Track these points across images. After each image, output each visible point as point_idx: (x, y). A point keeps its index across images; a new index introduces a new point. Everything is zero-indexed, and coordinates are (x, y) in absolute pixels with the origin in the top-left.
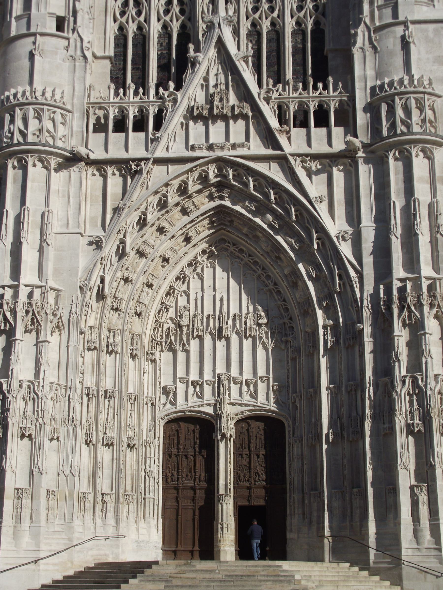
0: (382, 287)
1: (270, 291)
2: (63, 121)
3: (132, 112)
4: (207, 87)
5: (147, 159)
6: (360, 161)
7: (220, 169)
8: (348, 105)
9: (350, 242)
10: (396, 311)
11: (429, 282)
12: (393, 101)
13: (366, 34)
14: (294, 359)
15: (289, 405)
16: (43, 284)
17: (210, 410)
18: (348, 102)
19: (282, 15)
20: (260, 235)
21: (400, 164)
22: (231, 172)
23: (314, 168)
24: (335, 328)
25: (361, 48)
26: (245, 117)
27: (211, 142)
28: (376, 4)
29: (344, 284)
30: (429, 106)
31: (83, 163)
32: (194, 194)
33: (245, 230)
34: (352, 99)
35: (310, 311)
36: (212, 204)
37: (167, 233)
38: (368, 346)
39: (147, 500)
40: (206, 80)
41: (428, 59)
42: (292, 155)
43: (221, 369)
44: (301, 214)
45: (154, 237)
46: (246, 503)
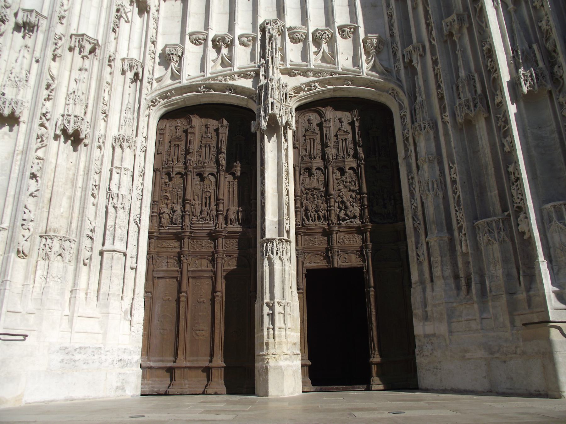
15: (398, 71)
39: (106, 255)
46: (321, 263)
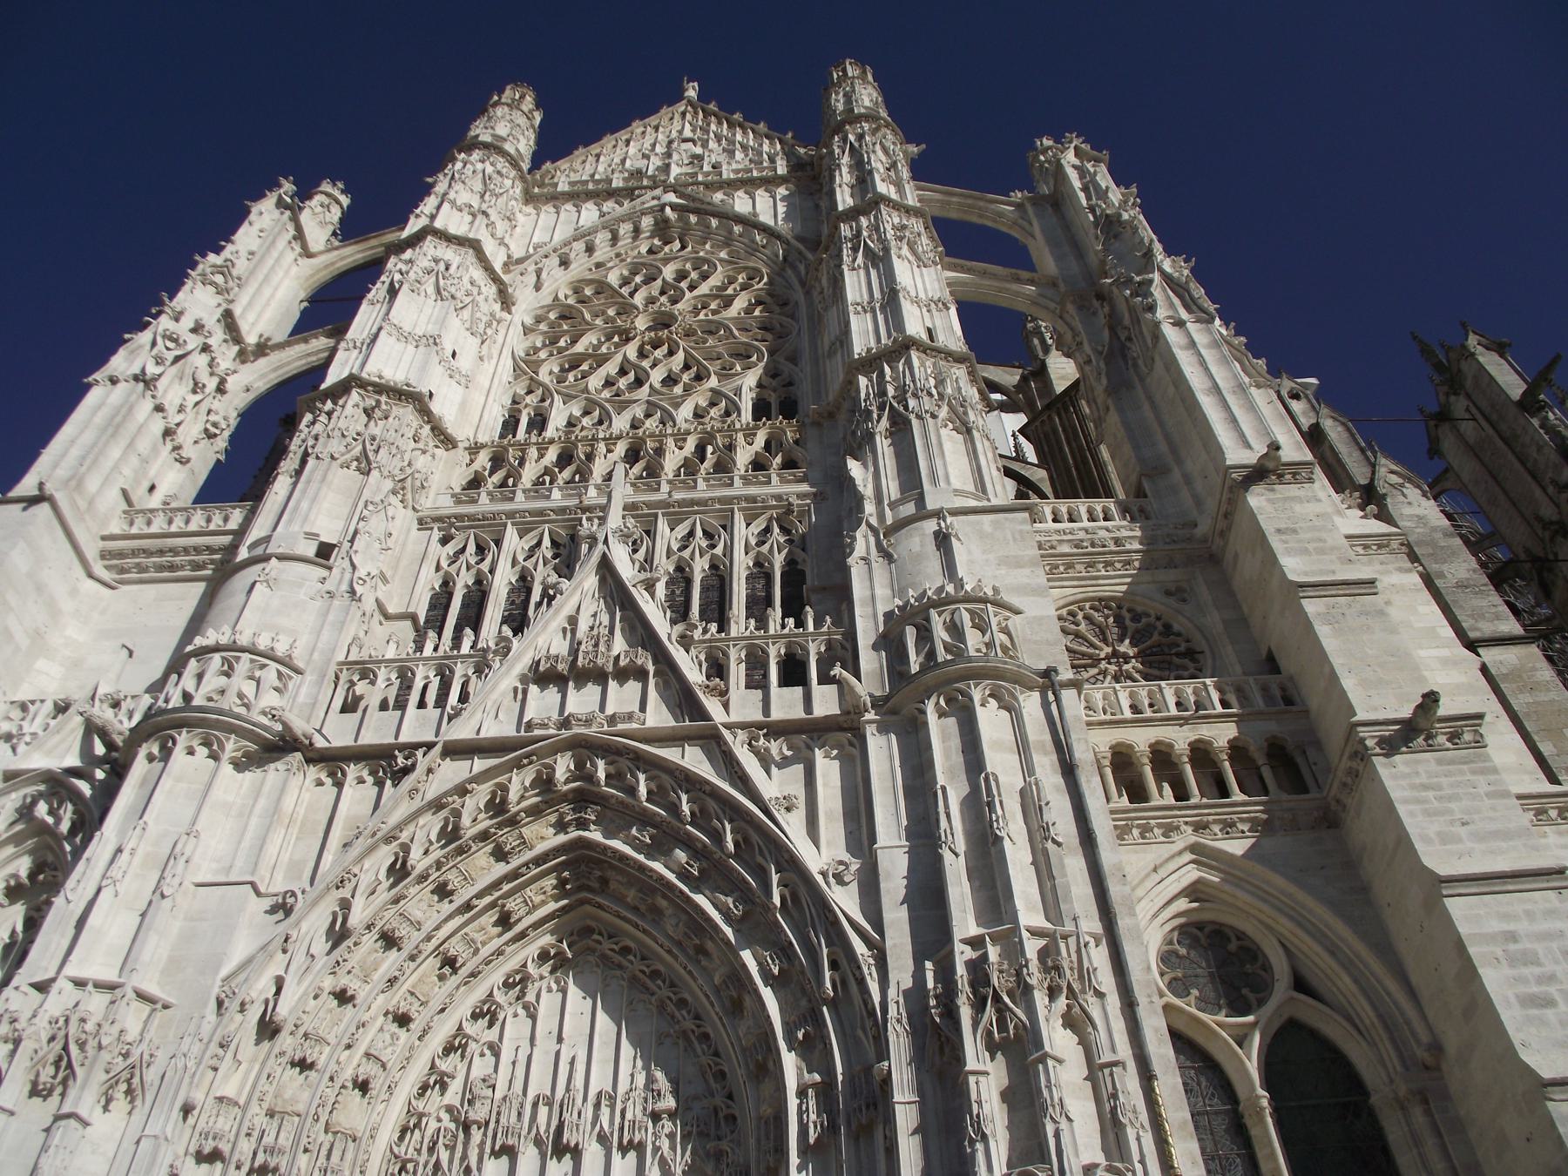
0: (929, 965)
2: (281, 686)
4: (574, 632)
5: (430, 746)
6: (870, 730)
7: (580, 765)
8: (843, 647)
9: (854, 887)
10: (966, 1013)
11: (1042, 942)
12: (928, 620)
13: (872, 540)
18: (844, 642)
19: (729, 550)
20: (664, 903)
21: (951, 722)
22: (601, 764)
23: (774, 752)
24: (826, 1092)
25: (863, 559)
26: (641, 675)
28: (886, 502)
29: (844, 982)
30: (999, 624)
31: (298, 755)
32: (523, 814)
34: (851, 636)
35: (771, 1064)
36: (562, 838)
37: (454, 898)
38: (906, 1117)
40: (573, 621)
42: (728, 726)
44: (746, 840)
45: (424, 906)
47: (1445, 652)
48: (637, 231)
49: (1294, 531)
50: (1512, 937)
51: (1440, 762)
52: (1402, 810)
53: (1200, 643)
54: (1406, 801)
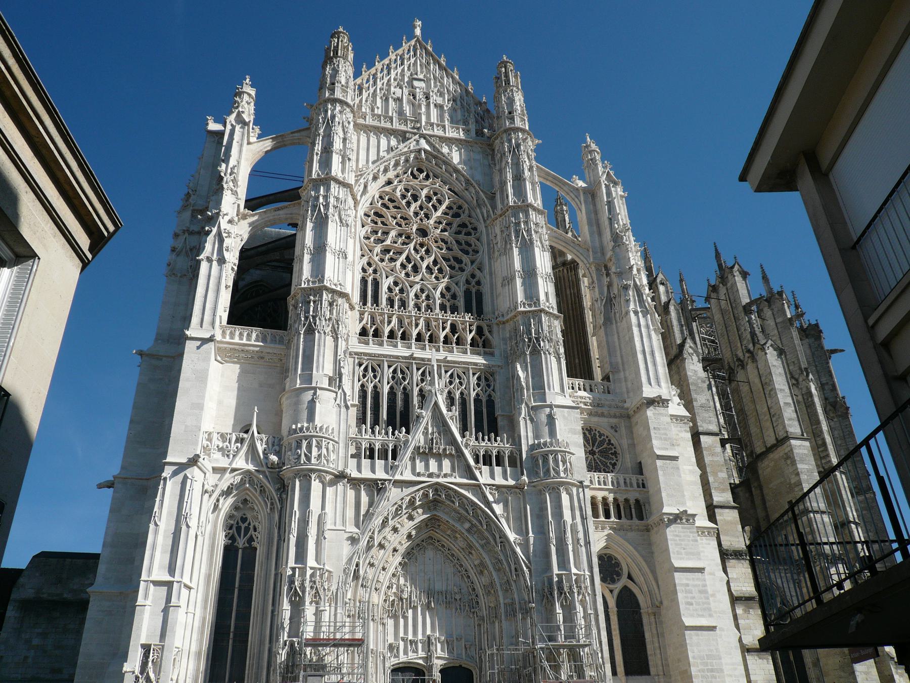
1: (462, 575)
3: (377, 446)
4: (427, 433)
5: (390, 480)
11: (575, 577)
14: (479, 625)
16: (322, 567)
17: (421, 662)
19: (468, 388)
25: (524, 418)
27: (431, 471)
33: (449, 532)
40: (426, 429)
41: (565, 429)
42: (484, 485)
43: (429, 632)
47: (691, 468)
48: (407, 161)
49: (659, 429)
50: (687, 585)
51: (682, 528)
52: (670, 542)
53: (619, 451)
54: (671, 540)
